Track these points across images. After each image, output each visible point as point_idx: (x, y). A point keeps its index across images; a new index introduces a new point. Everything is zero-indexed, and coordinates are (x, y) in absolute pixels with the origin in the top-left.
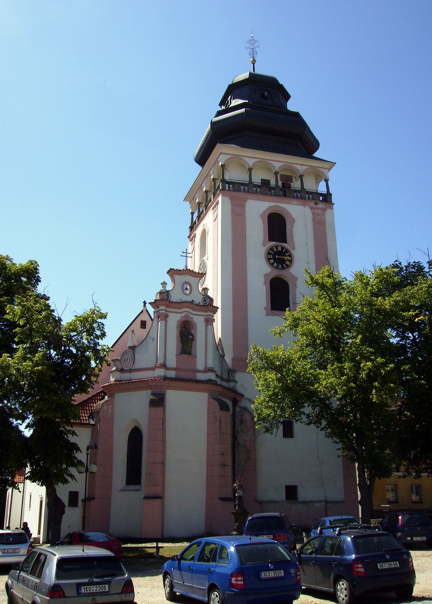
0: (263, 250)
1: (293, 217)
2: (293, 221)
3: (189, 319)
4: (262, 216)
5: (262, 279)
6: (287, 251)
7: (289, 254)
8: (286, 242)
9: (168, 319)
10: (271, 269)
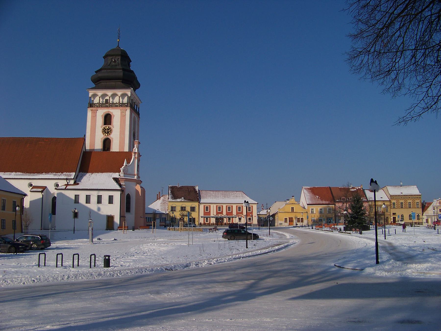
0: (101, 129)
2: (114, 116)
6: (110, 128)
7: (111, 129)
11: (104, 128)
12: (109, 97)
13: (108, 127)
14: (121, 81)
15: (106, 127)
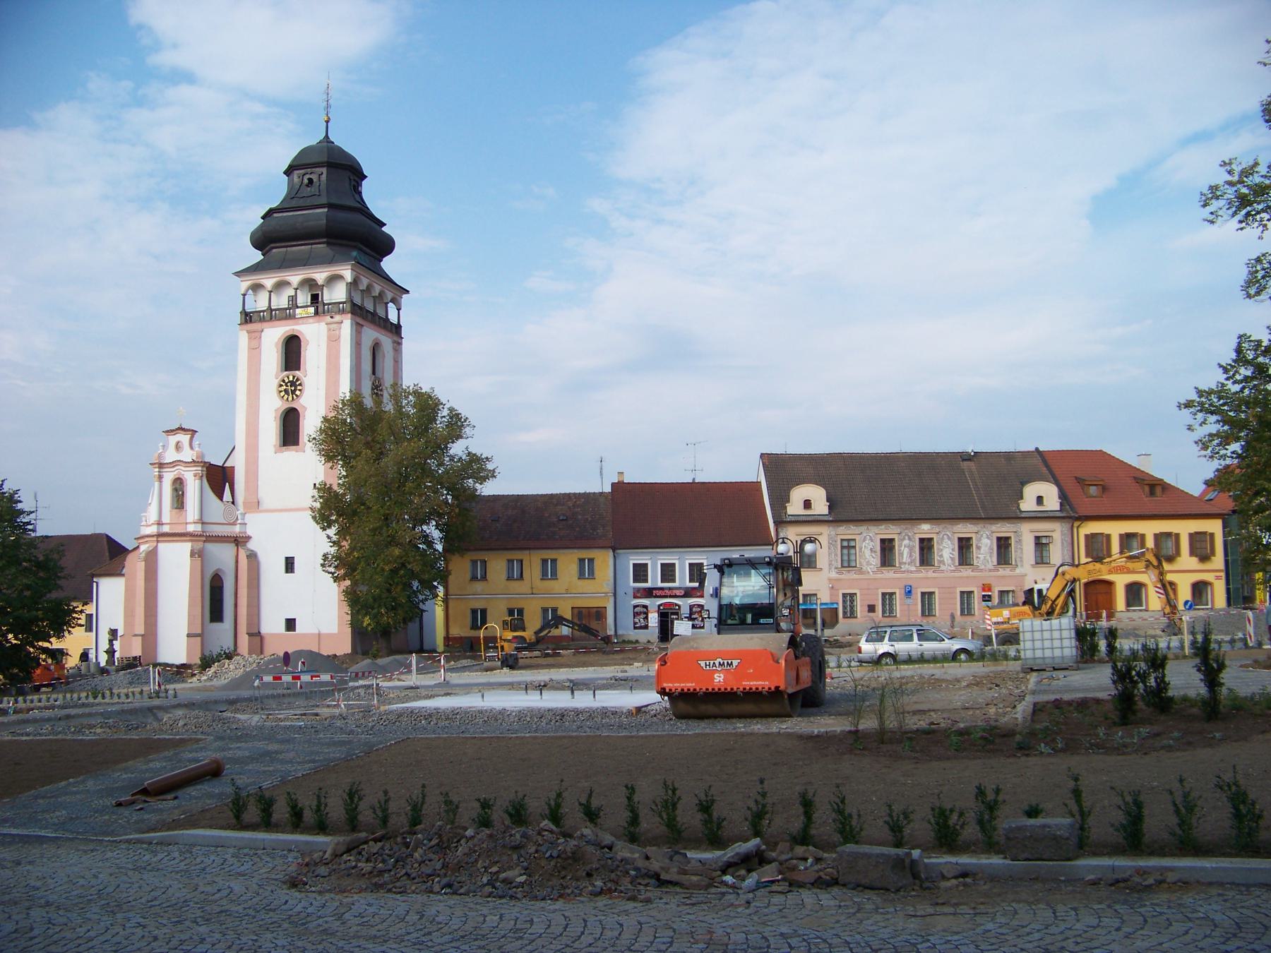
0: (276, 382)
3: (181, 477)
4: (277, 344)
8: (298, 369)
9: (163, 479)
10: (281, 403)
11: (284, 381)
13: (294, 377)
14: (325, 240)
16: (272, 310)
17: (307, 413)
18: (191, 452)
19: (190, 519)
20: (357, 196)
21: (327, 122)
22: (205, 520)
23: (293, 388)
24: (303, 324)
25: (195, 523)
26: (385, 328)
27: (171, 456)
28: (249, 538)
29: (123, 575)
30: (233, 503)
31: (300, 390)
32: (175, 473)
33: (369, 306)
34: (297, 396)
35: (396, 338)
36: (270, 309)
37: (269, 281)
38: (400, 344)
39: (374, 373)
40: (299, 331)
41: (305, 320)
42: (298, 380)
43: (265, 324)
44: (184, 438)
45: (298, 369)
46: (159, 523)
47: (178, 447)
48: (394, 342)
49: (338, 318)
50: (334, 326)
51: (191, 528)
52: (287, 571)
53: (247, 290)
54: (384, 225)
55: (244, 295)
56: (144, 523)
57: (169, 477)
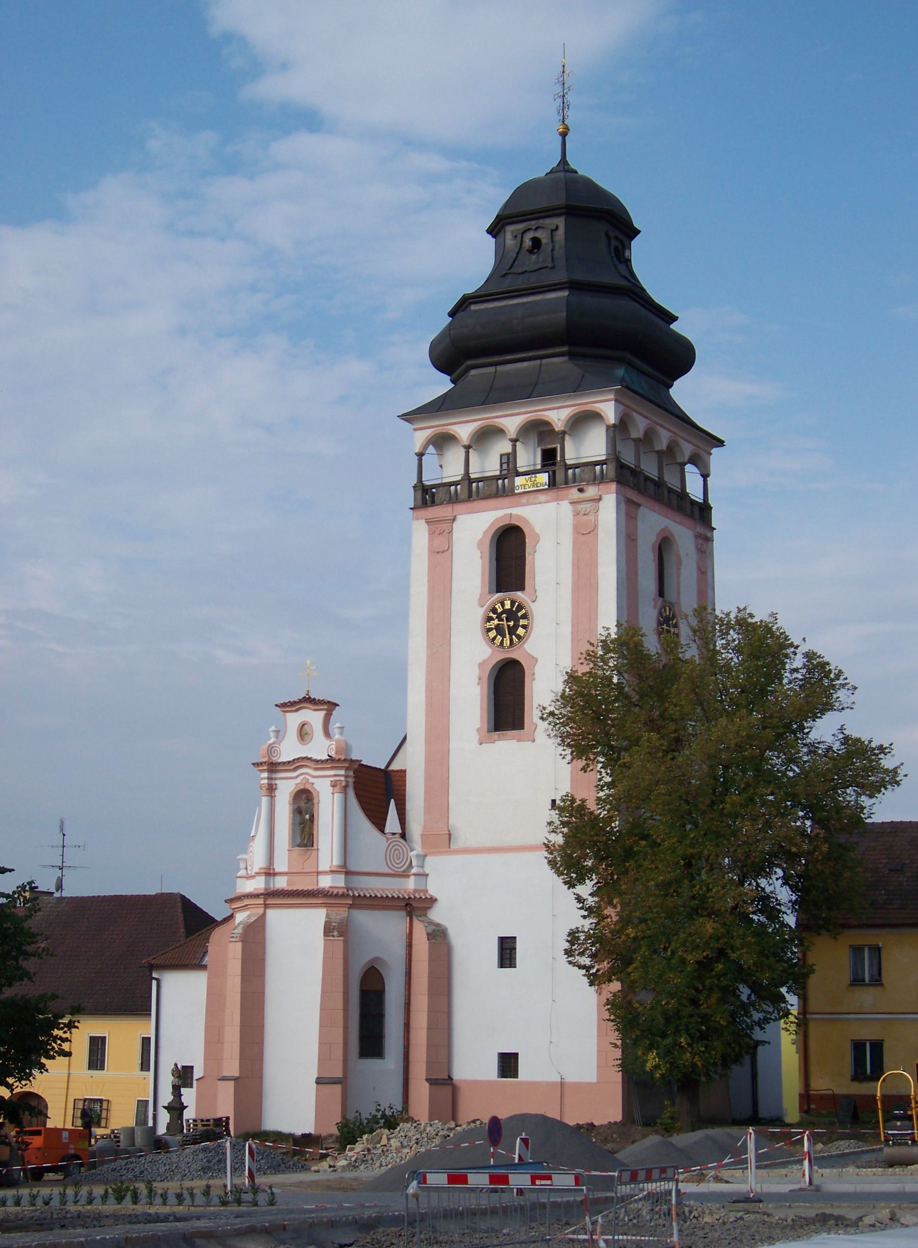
0: (480, 613)
1: (537, 530)
2: (537, 538)
3: (308, 787)
4: (480, 544)
5: (476, 672)
6: (520, 607)
8: (522, 588)
9: (277, 793)
11: (494, 610)
12: (511, 440)
13: (513, 603)
14: (565, 349)
15: (503, 605)
16: (471, 481)
17: (538, 669)
18: (327, 742)
19: (324, 865)
20: (621, 268)
21: (564, 135)
22: (352, 867)
23: (512, 623)
24: (527, 504)
25: (332, 872)
26: (680, 509)
27: (289, 750)
28: (433, 900)
29: (204, 967)
30: (403, 836)
31: (524, 627)
32: (298, 780)
33: (650, 468)
34: (519, 637)
35: (701, 530)
36: (467, 479)
37: (464, 430)
38: (709, 540)
39: (661, 593)
40: (520, 517)
41: (532, 497)
42: (520, 607)
43: (459, 507)
44: (315, 717)
45: (522, 588)
46: (269, 873)
47: (303, 733)
48: (698, 536)
49: (592, 491)
50: (587, 506)
51: (325, 882)
52: (502, 965)
53: (426, 447)
54: (675, 319)
55: (420, 455)
56: (242, 872)
57: (286, 787)
